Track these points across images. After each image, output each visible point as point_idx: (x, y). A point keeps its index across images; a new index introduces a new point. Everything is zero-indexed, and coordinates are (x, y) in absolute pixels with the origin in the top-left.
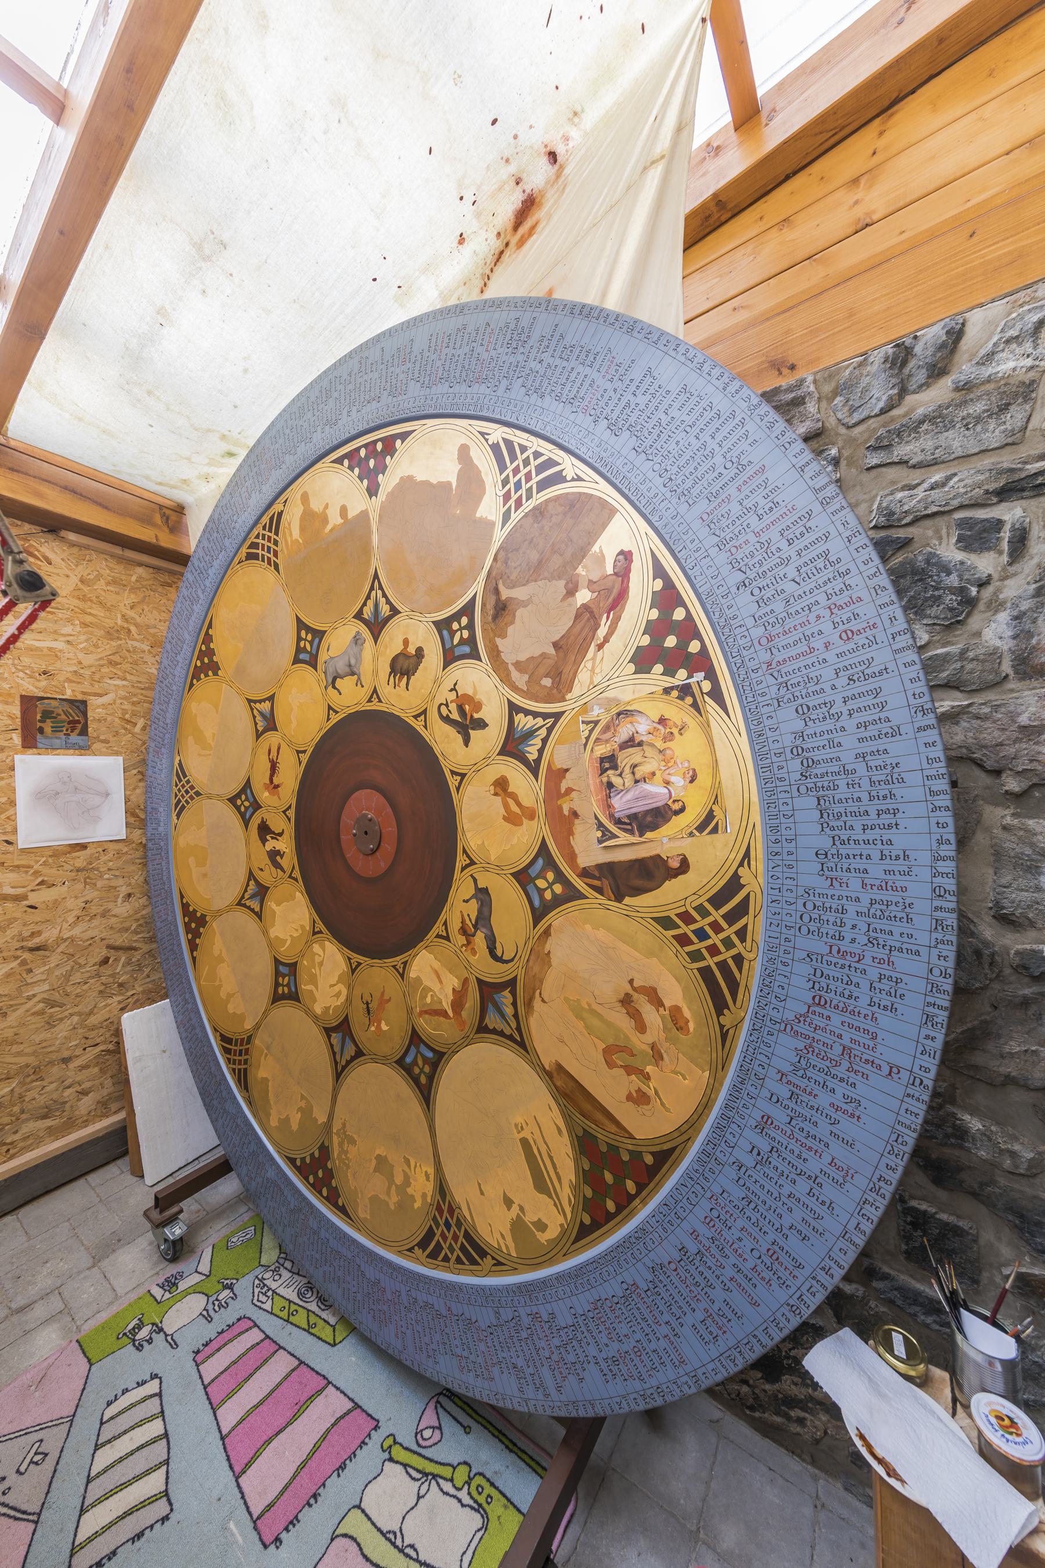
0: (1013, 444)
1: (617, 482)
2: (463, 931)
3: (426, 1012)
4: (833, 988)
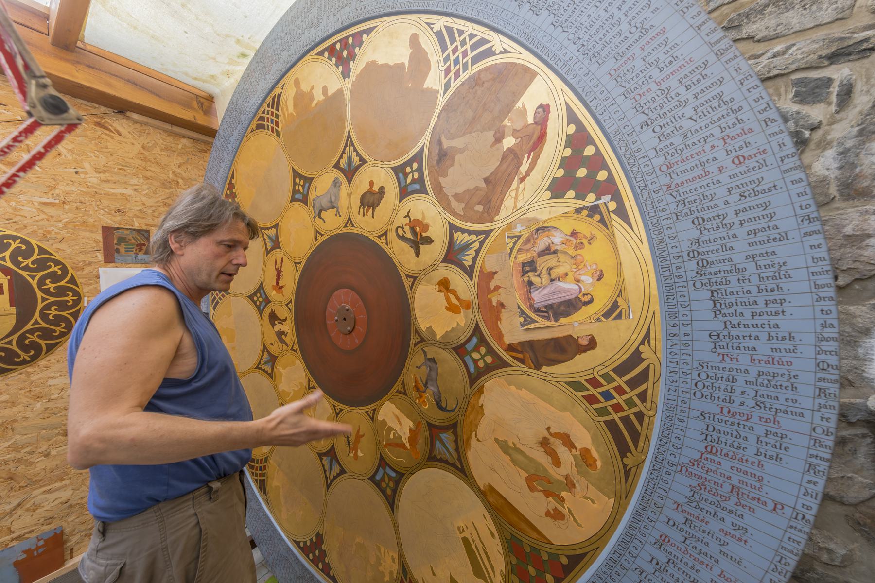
0: (843, 19)
1: (538, 51)
3: (390, 445)
4: (724, 440)
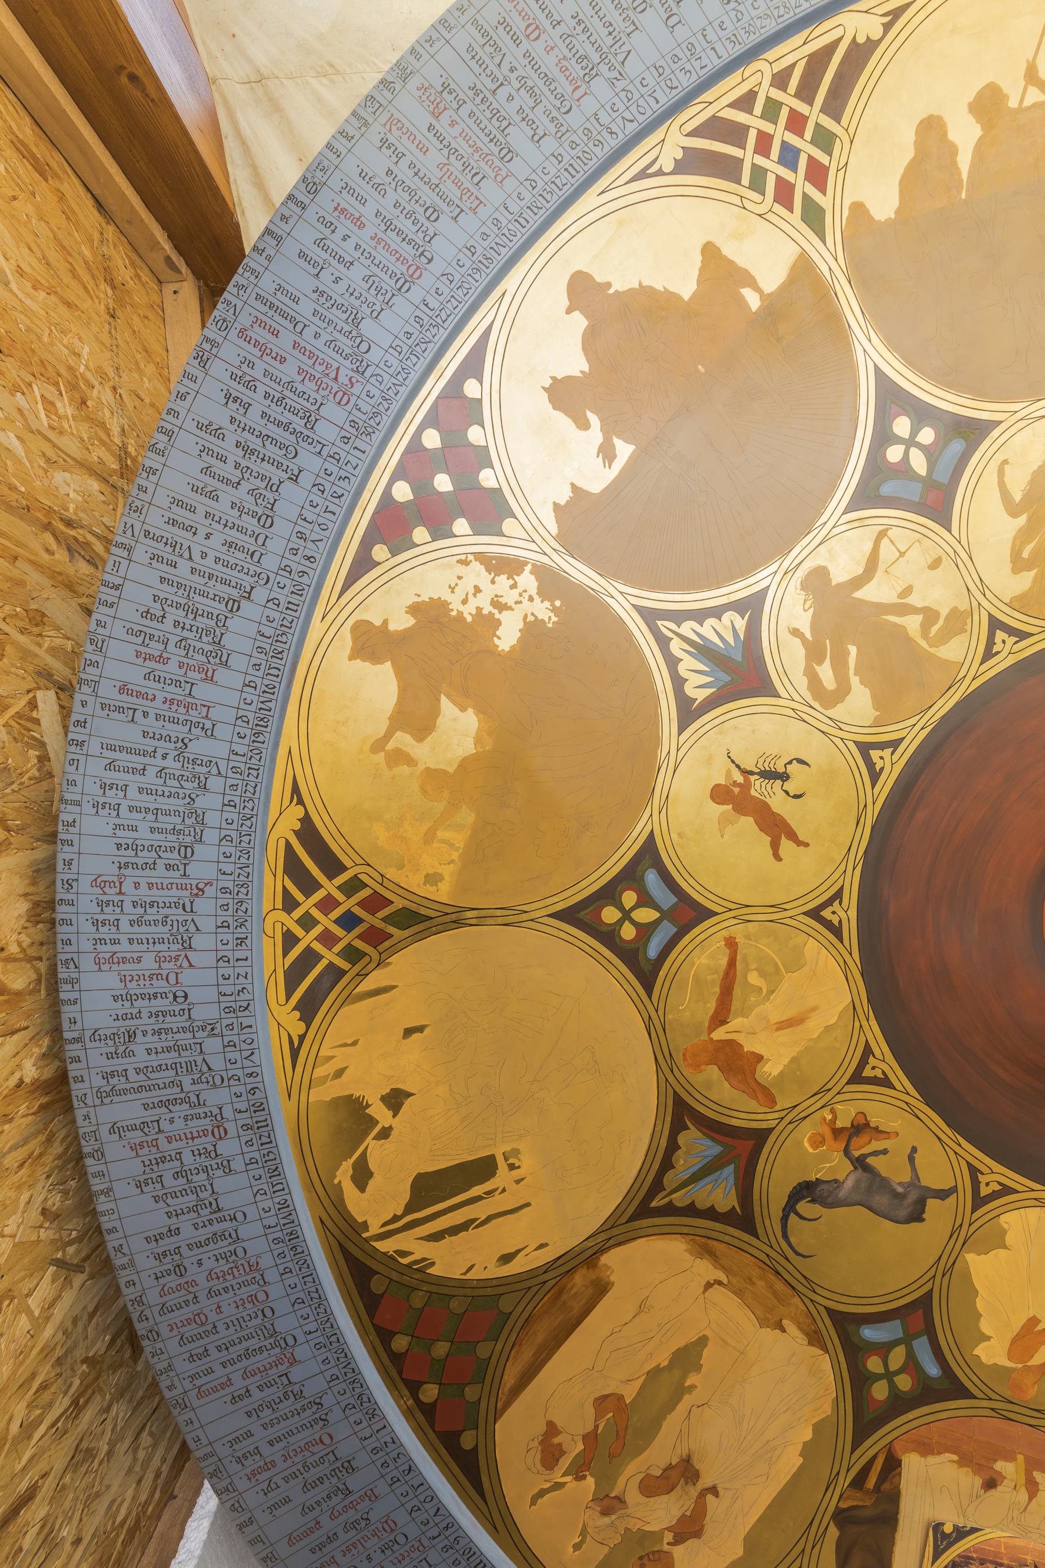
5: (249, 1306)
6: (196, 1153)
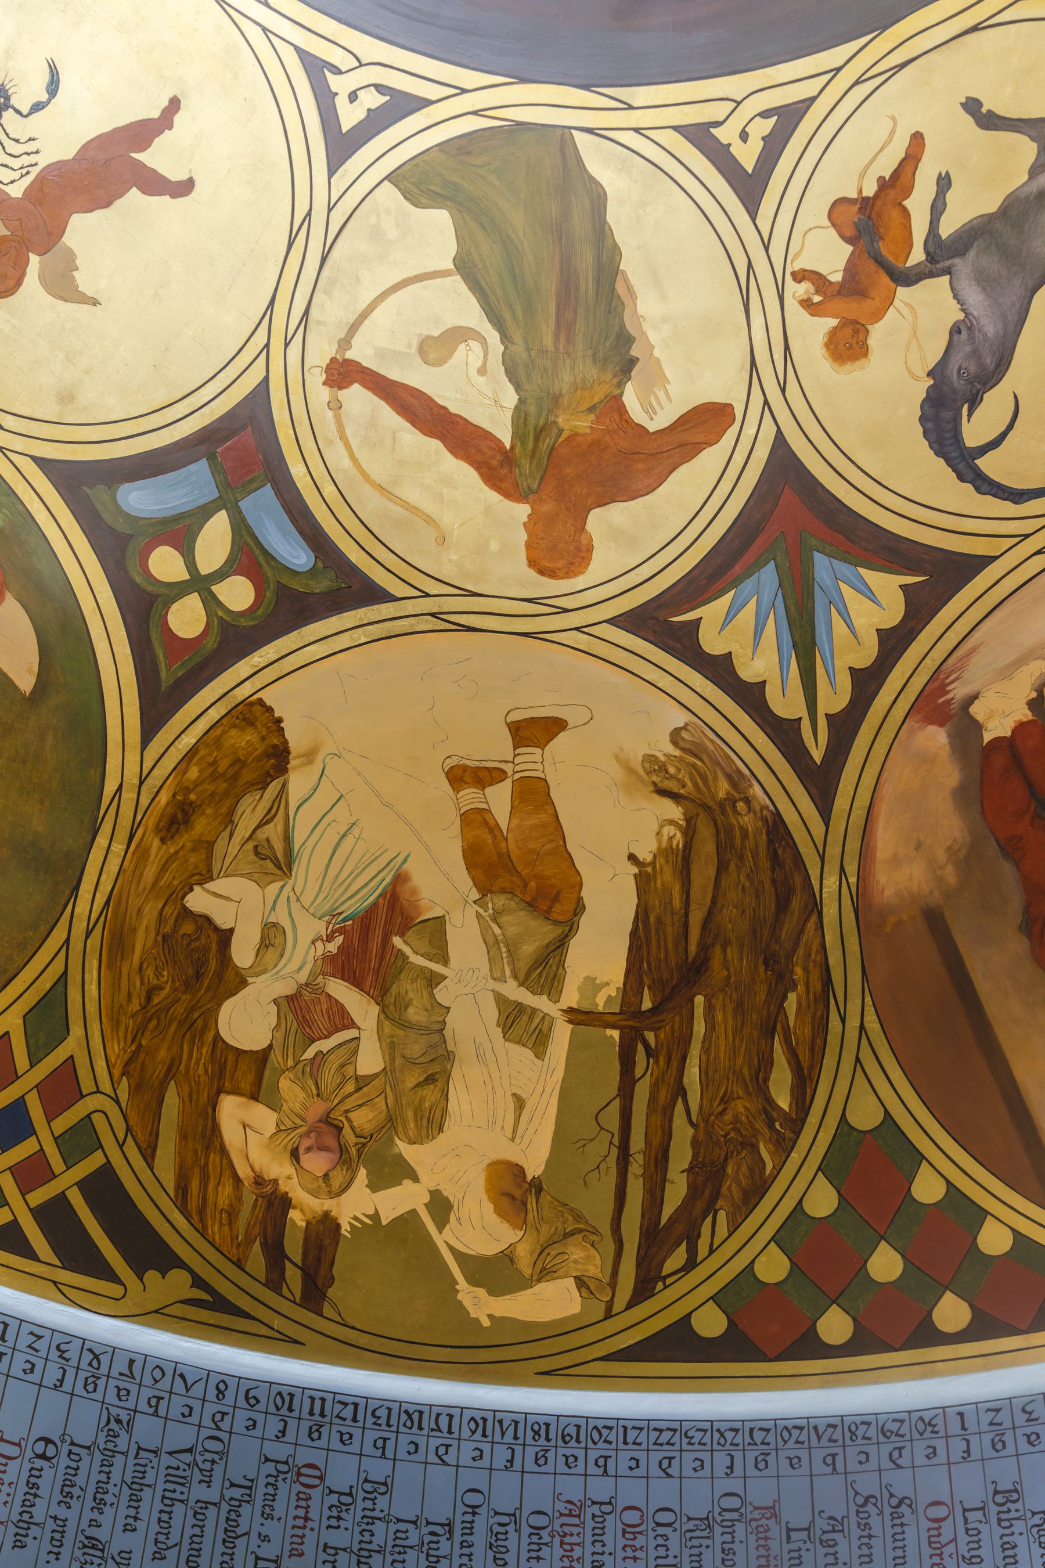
2: (869, 218)
5: (640, 1541)
6: (333, 1522)
